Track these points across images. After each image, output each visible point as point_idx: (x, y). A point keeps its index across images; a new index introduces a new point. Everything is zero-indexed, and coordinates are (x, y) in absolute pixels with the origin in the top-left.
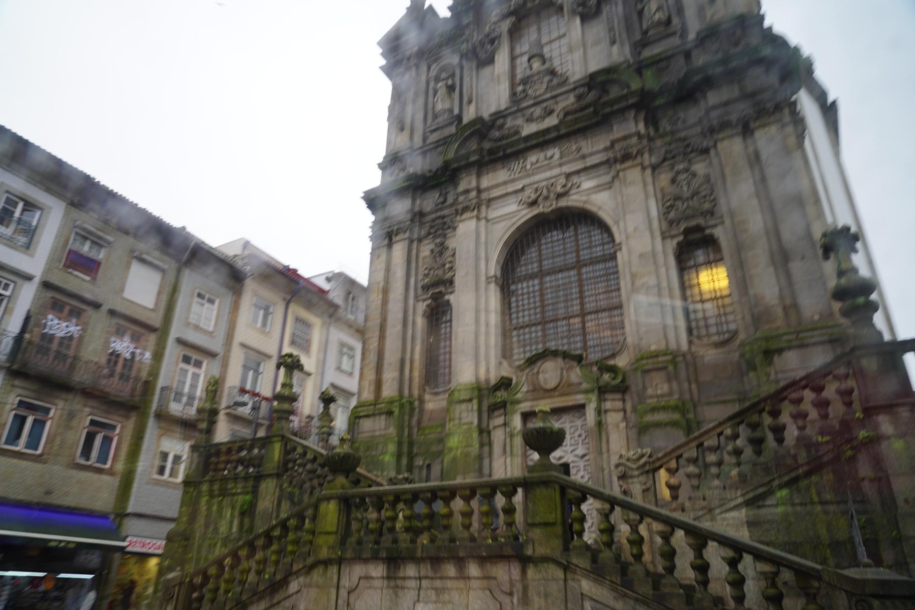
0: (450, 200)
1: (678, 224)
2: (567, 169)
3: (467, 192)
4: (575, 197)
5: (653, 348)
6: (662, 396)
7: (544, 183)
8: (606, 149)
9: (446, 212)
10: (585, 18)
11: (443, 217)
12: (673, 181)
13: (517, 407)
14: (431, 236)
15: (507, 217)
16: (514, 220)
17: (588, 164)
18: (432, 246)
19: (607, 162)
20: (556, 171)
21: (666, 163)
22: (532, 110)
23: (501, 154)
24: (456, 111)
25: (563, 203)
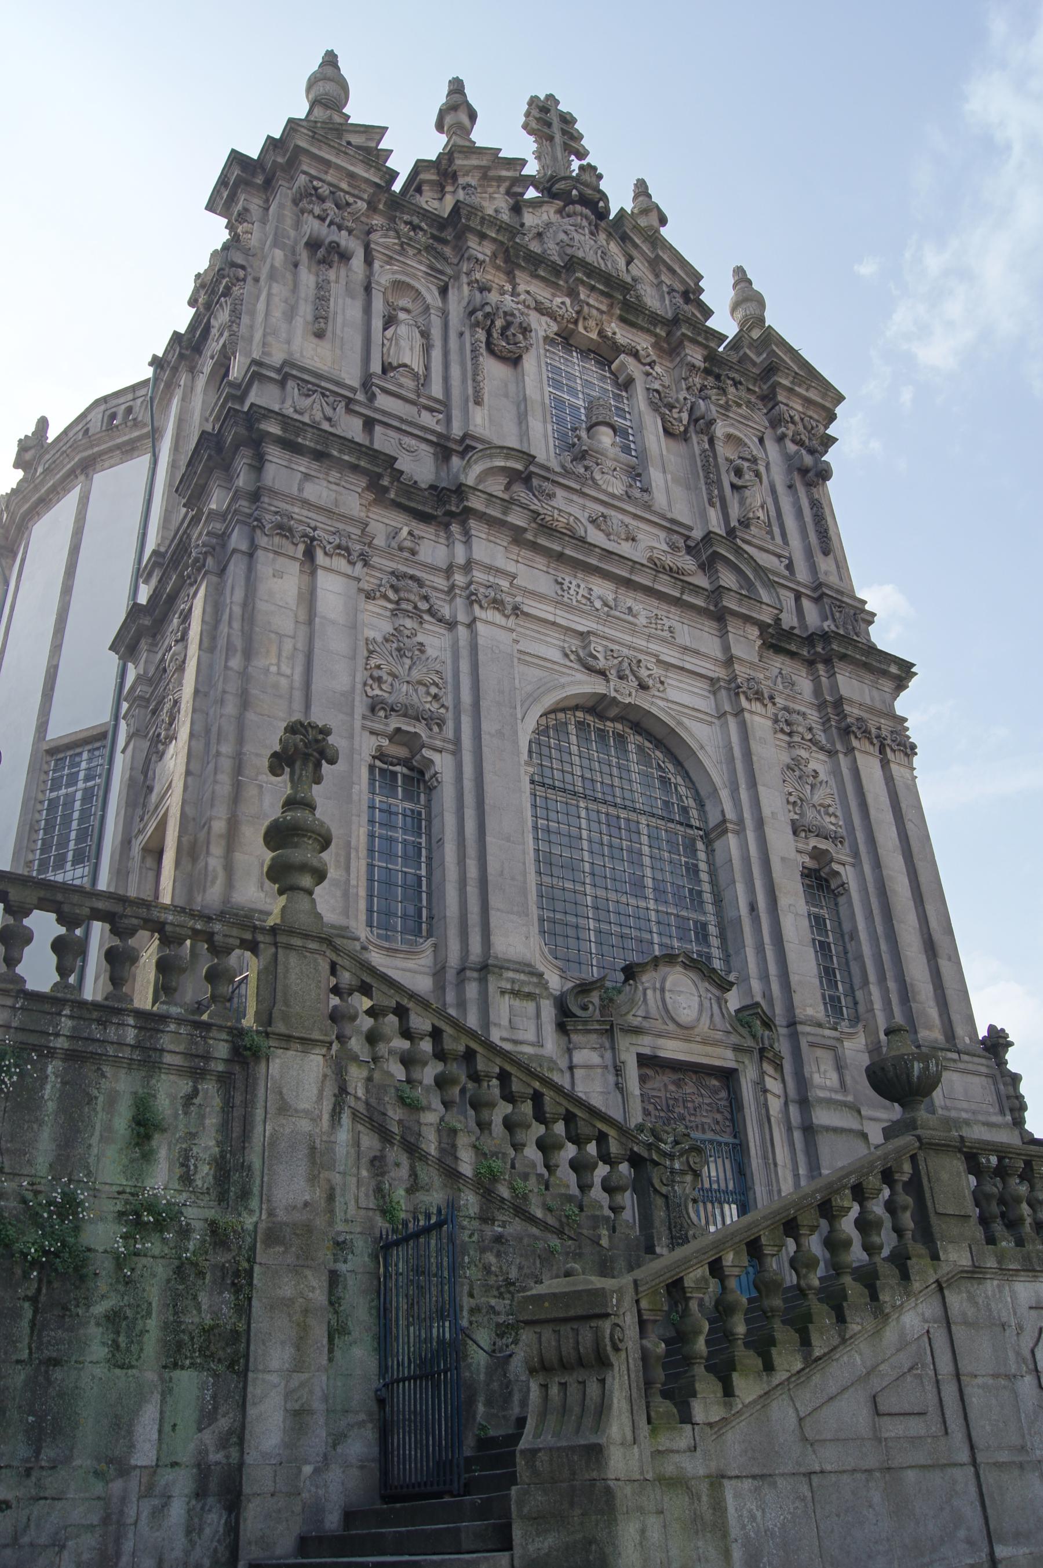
1: (806, 838)
3: (499, 571)
5: (810, 1011)
6: (831, 1090)
7: (625, 651)
13: (634, 1039)
14: (390, 606)
15: (549, 665)
16: (564, 680)
17: (688, 666)
18: (387, 627)
22: (601, 509)
25: (642, 701)
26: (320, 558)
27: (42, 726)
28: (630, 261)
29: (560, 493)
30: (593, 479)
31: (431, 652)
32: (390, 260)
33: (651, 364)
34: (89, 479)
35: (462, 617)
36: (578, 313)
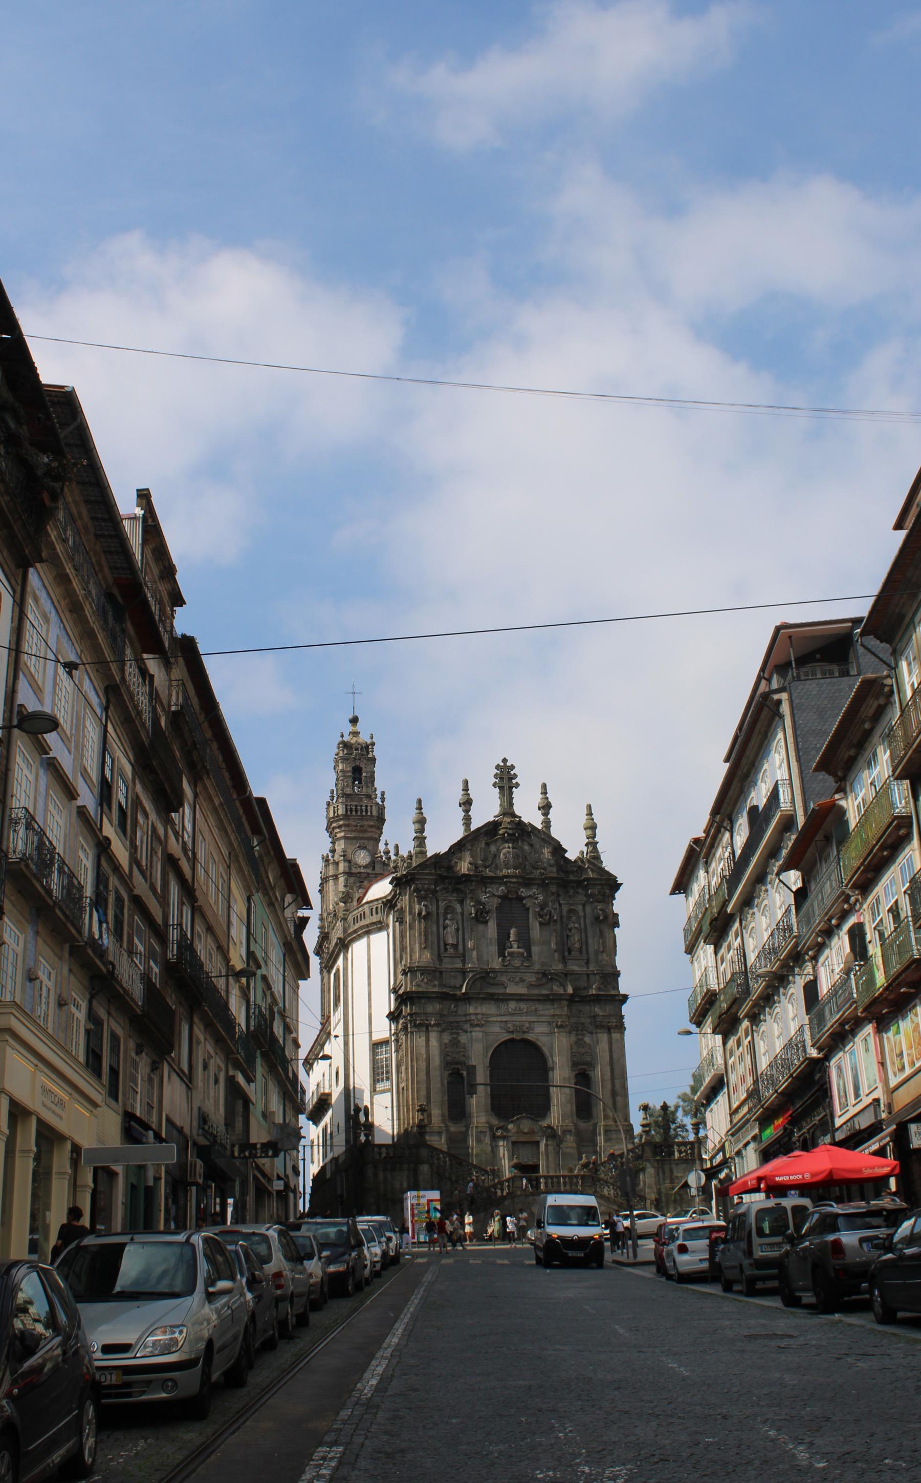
0: (460, 1012)
2: (529, 1018)
4: (531, 1035)
8: (550, 1016)
9: (458, 1019)
10: (541, 924)
11: (458, 1022)
12: (576, 1043)
18: (450, 1038)
19: (549, 1022)
20: (524, 1018)
21: (575, 1032)
23: (496, 997)
24: (460, 947)
25: (526, 1036)
26: (430, 1029)
27: (370, 1033)
28: (531, 845)
29: (499, 974)
30: (510, 963)
31: (462, 1041)
32: (444, 900)
33: (537, 898)
34: (368, 937)
35: (469, 1030)
36: (508, 891)
